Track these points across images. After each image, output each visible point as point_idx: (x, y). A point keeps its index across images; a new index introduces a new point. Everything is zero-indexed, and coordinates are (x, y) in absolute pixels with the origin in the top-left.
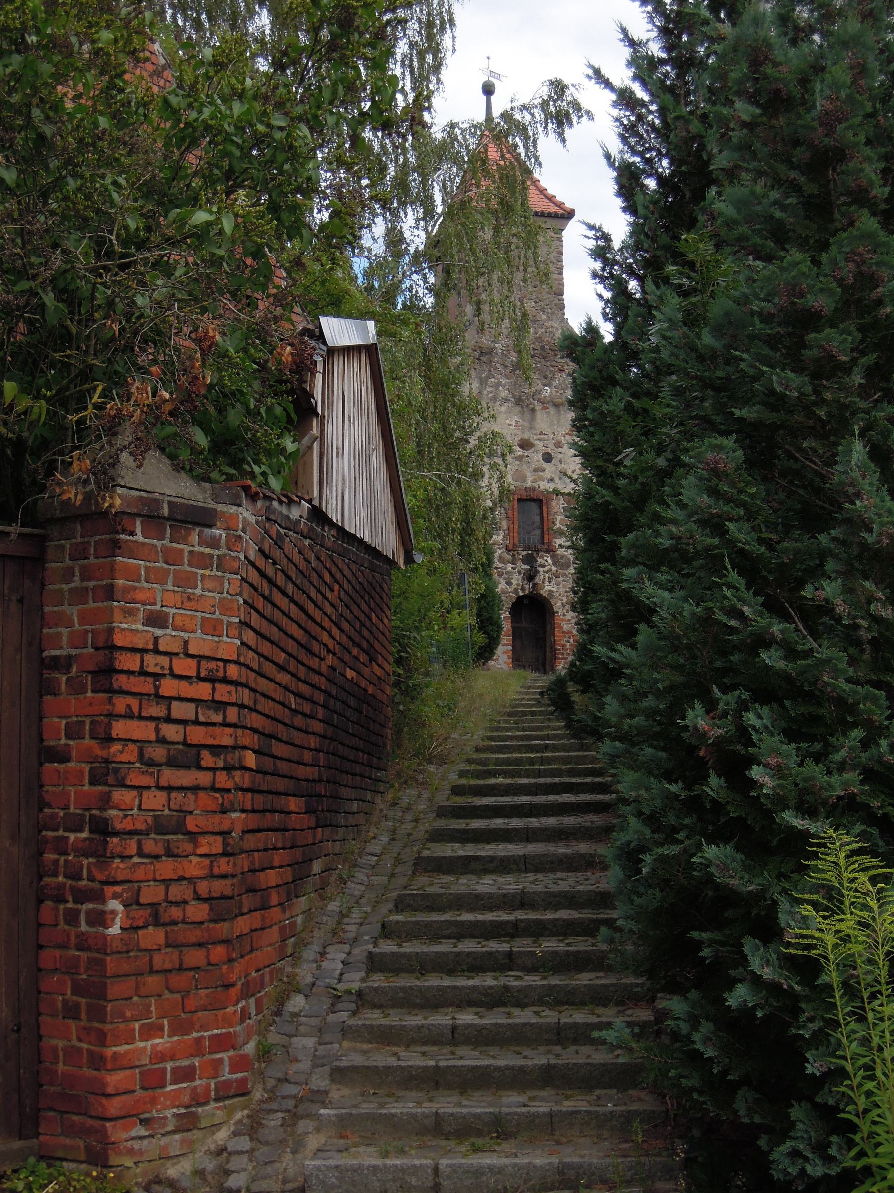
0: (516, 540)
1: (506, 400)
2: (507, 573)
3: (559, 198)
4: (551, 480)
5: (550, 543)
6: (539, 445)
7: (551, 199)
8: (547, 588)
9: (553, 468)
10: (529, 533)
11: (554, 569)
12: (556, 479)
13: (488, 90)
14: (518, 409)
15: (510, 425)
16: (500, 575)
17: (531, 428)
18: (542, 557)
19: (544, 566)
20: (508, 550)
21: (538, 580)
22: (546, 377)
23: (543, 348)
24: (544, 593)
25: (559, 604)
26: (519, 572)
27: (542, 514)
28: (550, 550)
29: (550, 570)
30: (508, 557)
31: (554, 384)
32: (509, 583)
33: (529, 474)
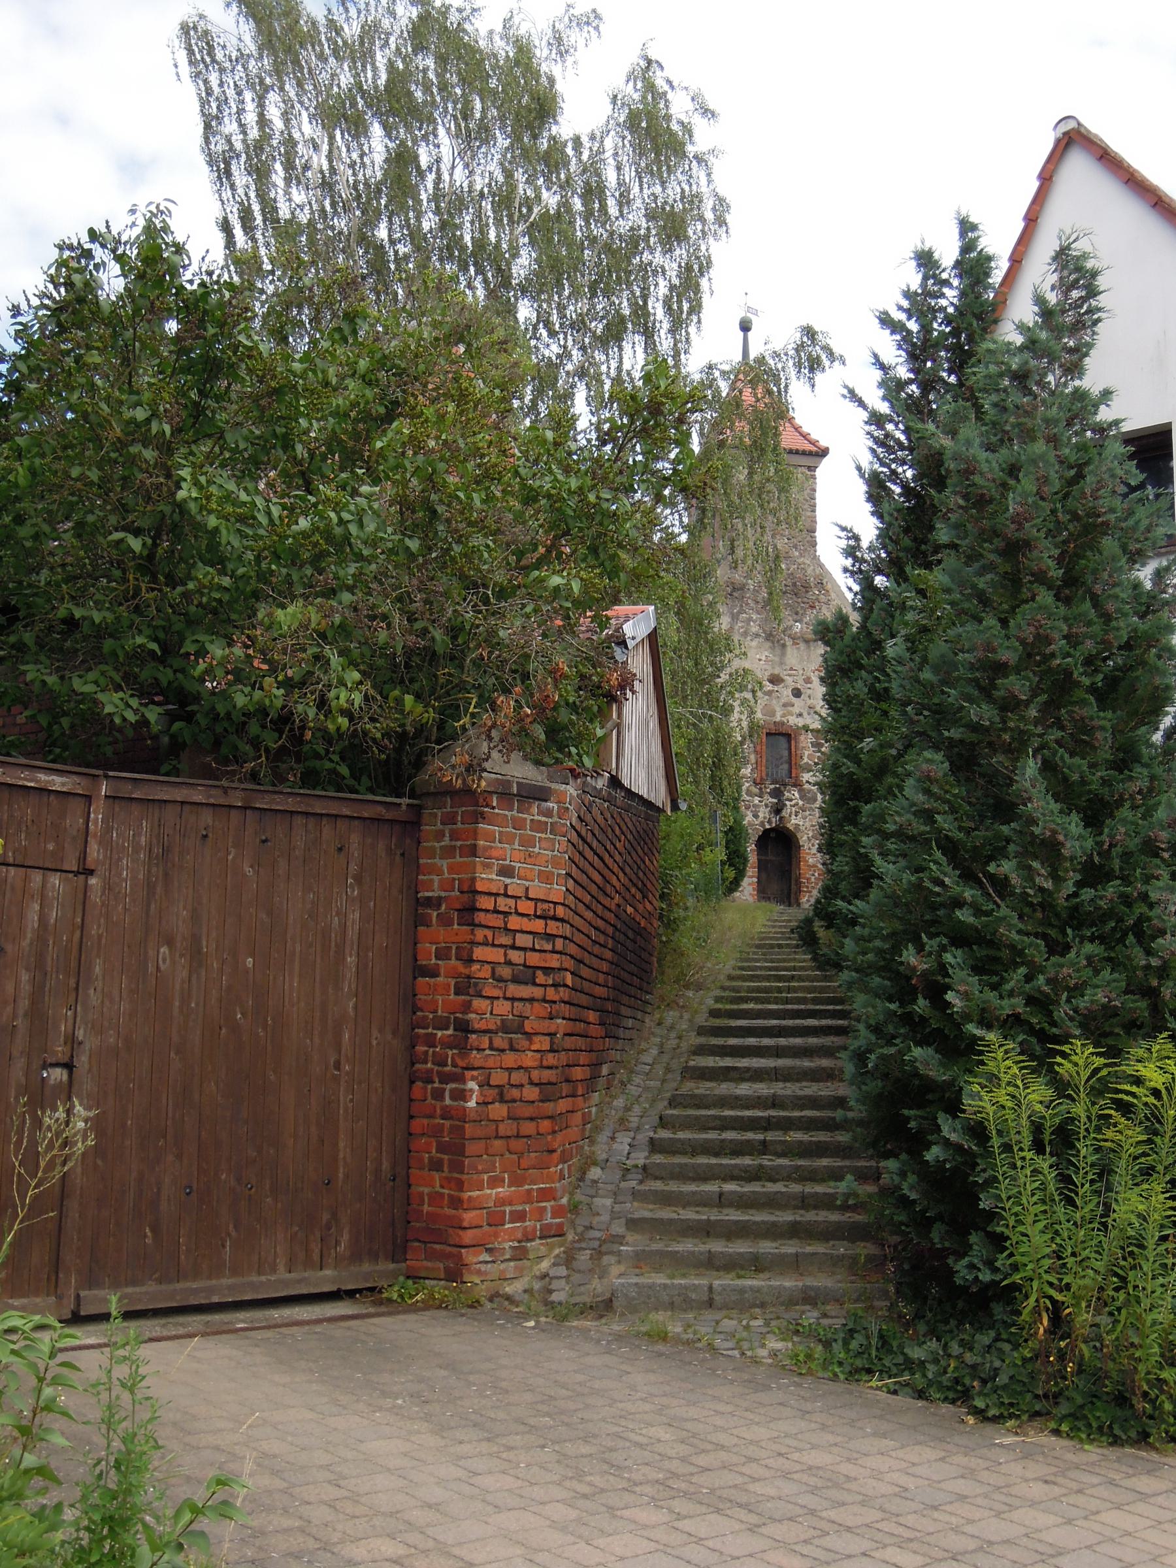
1: (757, 635)
3: (814, 436)
4: (800, 715)
6: (789, 680)
7: (805, 436)
13: (745, 327)
14: (769, 644)
16: (747, 808)
20: (755, 783)
21: (784, 814)
23: (794, 584)
24: (790, 826)
27: (790, 749)
28: (797, 784)
30: (755, 790)
32: (756, 816)
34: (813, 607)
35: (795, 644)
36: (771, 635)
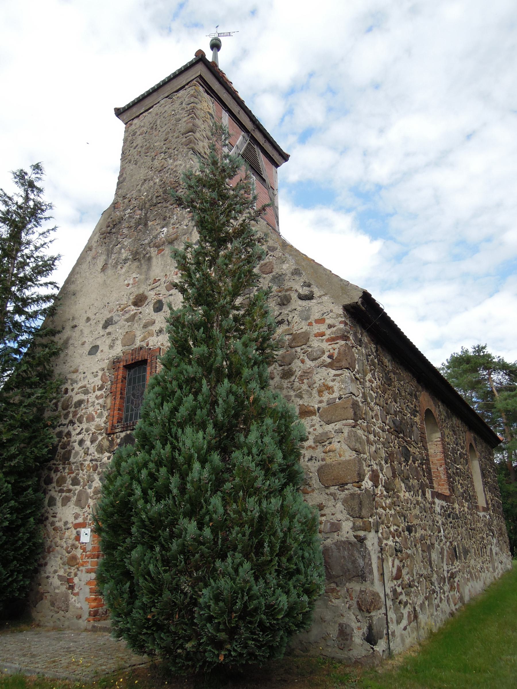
0: (115, 421)
14: (136, 264)
36: (137, 253)
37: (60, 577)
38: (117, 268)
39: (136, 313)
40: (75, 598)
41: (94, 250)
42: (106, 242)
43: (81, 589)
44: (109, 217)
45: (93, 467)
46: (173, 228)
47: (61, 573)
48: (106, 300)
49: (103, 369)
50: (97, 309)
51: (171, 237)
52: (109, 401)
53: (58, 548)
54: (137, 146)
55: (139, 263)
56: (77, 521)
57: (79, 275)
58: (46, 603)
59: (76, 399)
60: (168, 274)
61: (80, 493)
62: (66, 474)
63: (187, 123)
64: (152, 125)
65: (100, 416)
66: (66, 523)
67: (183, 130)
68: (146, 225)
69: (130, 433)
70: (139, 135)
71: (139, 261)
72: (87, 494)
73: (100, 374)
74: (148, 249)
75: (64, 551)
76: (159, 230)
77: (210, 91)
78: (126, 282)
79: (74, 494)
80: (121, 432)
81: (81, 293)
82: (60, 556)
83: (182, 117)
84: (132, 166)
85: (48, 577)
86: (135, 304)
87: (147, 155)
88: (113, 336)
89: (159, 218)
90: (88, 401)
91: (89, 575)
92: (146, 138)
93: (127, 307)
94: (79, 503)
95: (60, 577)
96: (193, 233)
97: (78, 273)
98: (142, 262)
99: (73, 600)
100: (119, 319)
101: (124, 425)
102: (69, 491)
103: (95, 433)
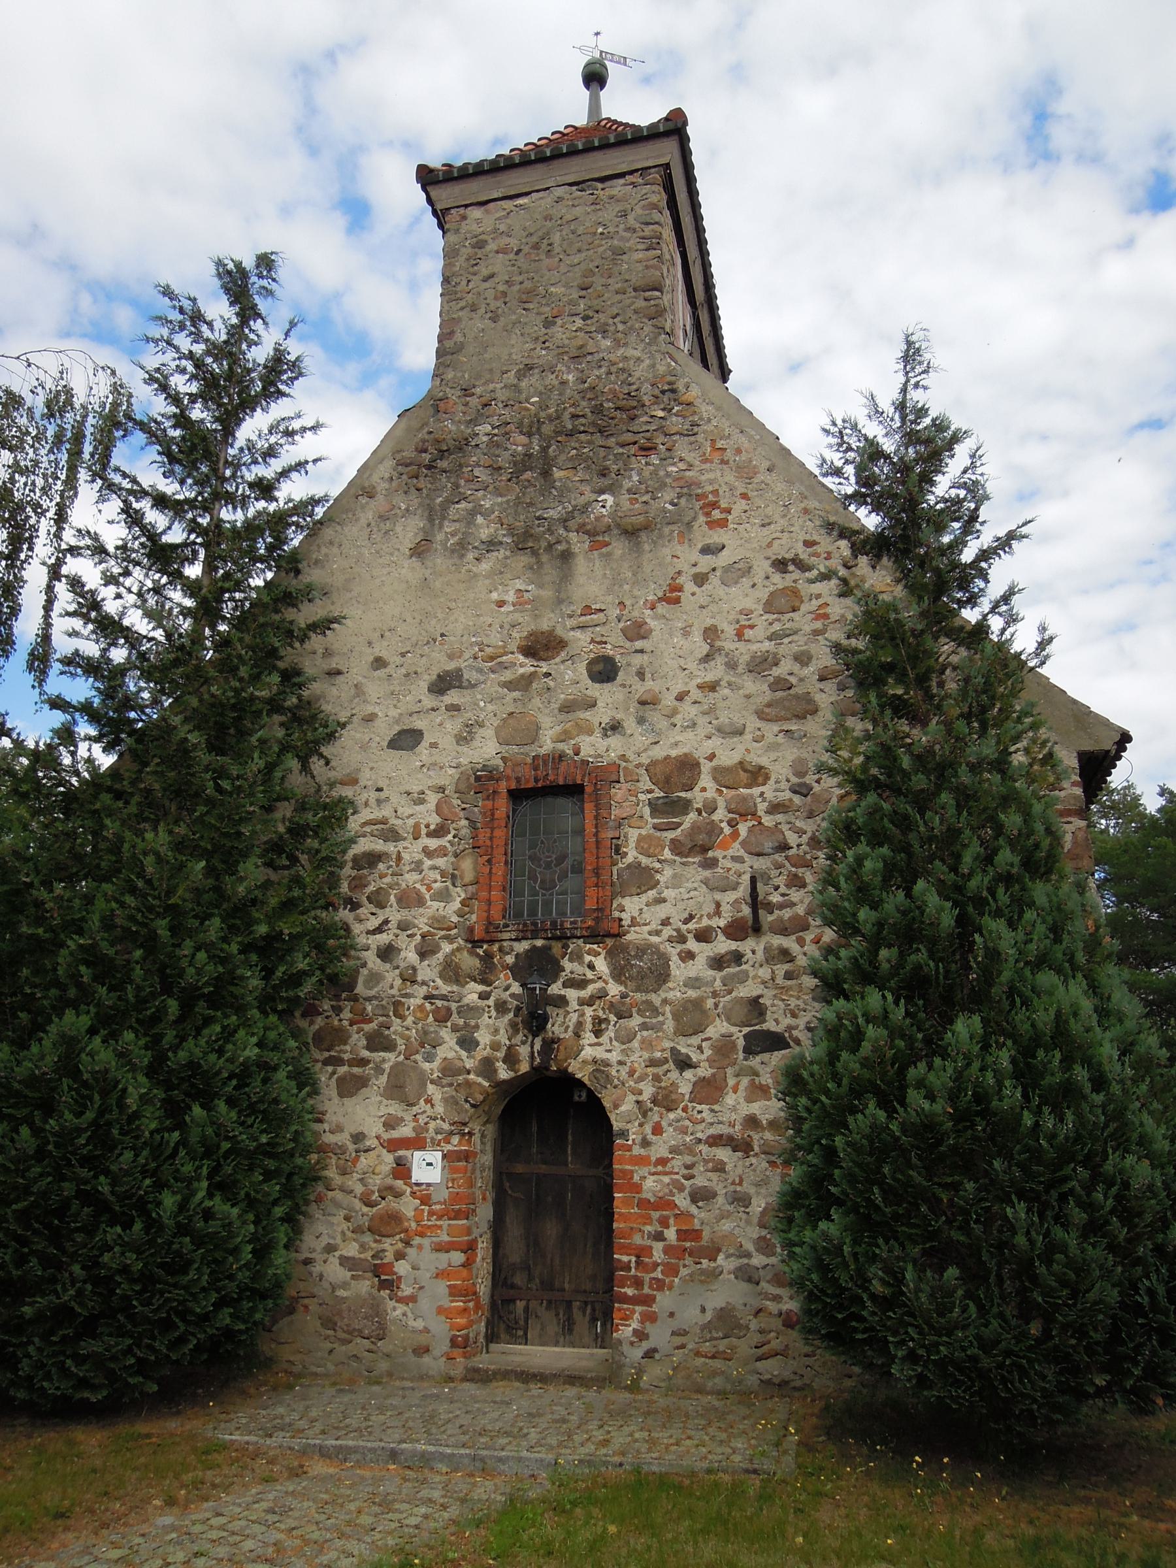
0: (496, 913)
1: (492, 545)
2: (467, 1011)
4: (615, 727)
5: (602, 911)
6: (581, 641)
8: (588, 1052)
9: (620, 695)
10: (548, 886)
11: (614, 989)
12: (630, 724)
14: (524, 559)
15: (501, 604)
17: (560, 601)
18: (577, 957)
19: (581, 984)
21: (557, 1027)
22: (603, 473)
23: (598, 410)
24: (579, 1069)
25: (628, 1105)
26: (501, 1007)
29: (601, 995)
30: (469, 962)
31: (627, 484)
32: (468, 1043)
33: (546, 721)
34: (647, 450)
35: (596, 546)
36: (527, 534)
37: (344, 1261)
38: (462, 556)
39: (533, 675)
40: (401, 1308)
41: (380, 498)
42: (420, 486)
43: (421, 1288)
44: (422, 427)
45: (433, 1012)
46: (633, 501)
47: (351, 1250)
48: (434, 626)
49: (441, 789)
50: (408, 643)
51: (628, 520)
52: (467, 866)
53: (338, 1195)
54: (492, 276)
55: (533, 560)
56: (395, 1134)
57: (335, 550)
58: (308, 1321)
59: (364, 845)
60: (628, 603)
61: (397, 1072)
62: (345, 1023)
63: (647, 267)
64: (535, 239)
65: (443, 896)
66: (358, 1137)
67: (635, 279)
68: (546, 474)
69: (544, 947)
70: (497, 252)
71: (535, 553)
72: (422, 1073)
73: (433, 798)
74: (561, 531)
75: (357, 1201)
76: (589, 496)
77: (672, 204)
78: (495, 596)
79: (379, 1070)
80: (517, 940)
81: (349, 595)
82: (342, 1213)
83: (630, 249)
84: (478, 323)
85: (307, 1262)
86: (530, 651)
87: (527, 306)
88: (469, 716)
89: (588, 468)
90: (399, 858)
91: (444, 1257)
92: (519, 264)
93: (506, 654)
94: (397, 1089)
95: (344, 1261)
96: (696, 525)
97: (331, 543)
98: (545, 558)
99: (398, 1312)
100: (482, 678)
101: (525, 925)
102: (363, 1062)
103: (429, 934)
